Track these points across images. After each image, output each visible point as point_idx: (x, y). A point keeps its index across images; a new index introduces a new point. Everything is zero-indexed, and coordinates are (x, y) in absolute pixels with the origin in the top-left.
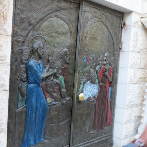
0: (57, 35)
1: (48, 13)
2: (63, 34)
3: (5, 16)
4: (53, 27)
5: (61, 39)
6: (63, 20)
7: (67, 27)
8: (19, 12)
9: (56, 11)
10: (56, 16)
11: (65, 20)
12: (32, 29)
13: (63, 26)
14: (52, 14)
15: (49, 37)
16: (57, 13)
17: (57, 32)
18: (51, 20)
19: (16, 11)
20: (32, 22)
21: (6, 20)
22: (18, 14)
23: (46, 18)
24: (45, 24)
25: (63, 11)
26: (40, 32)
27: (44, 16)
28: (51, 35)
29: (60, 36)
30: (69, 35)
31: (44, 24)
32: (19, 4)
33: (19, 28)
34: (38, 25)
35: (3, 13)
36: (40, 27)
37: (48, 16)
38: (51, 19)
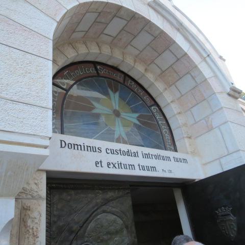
0: (109, 236)
1: (93, 211)
2: (117, 232)
3: (35, 233)
4: (102, 226)
5: (116, 241)
6: (114, 214)
7: (120, 221)
8: (56, 220)
9: (103, 205)
10: (104, 212)
11: (116, 213)
12: (75, 238)
13: (115, 221)
14: (99, 211)
15: (98, 242)
16: (104, 208)
17: (108, 233)
18: (98, 219)
19: (51, 220)
20: (74, 229)
21: (38, 237)
22: (55, 222)
23: (91, 218)
24: (92, 225)
25: (111, 202)
26: (86, 239)
27: (88, 216)
28: (101, 238)
29: (113, 236)
30: (125, 232)
31: (89, 227)
32: (55, 209)
33: (57, 242)
34: (82, 230)
35: (33, 229)
36: (85, 232)
37: (94, 215)
38: (98, 217)
